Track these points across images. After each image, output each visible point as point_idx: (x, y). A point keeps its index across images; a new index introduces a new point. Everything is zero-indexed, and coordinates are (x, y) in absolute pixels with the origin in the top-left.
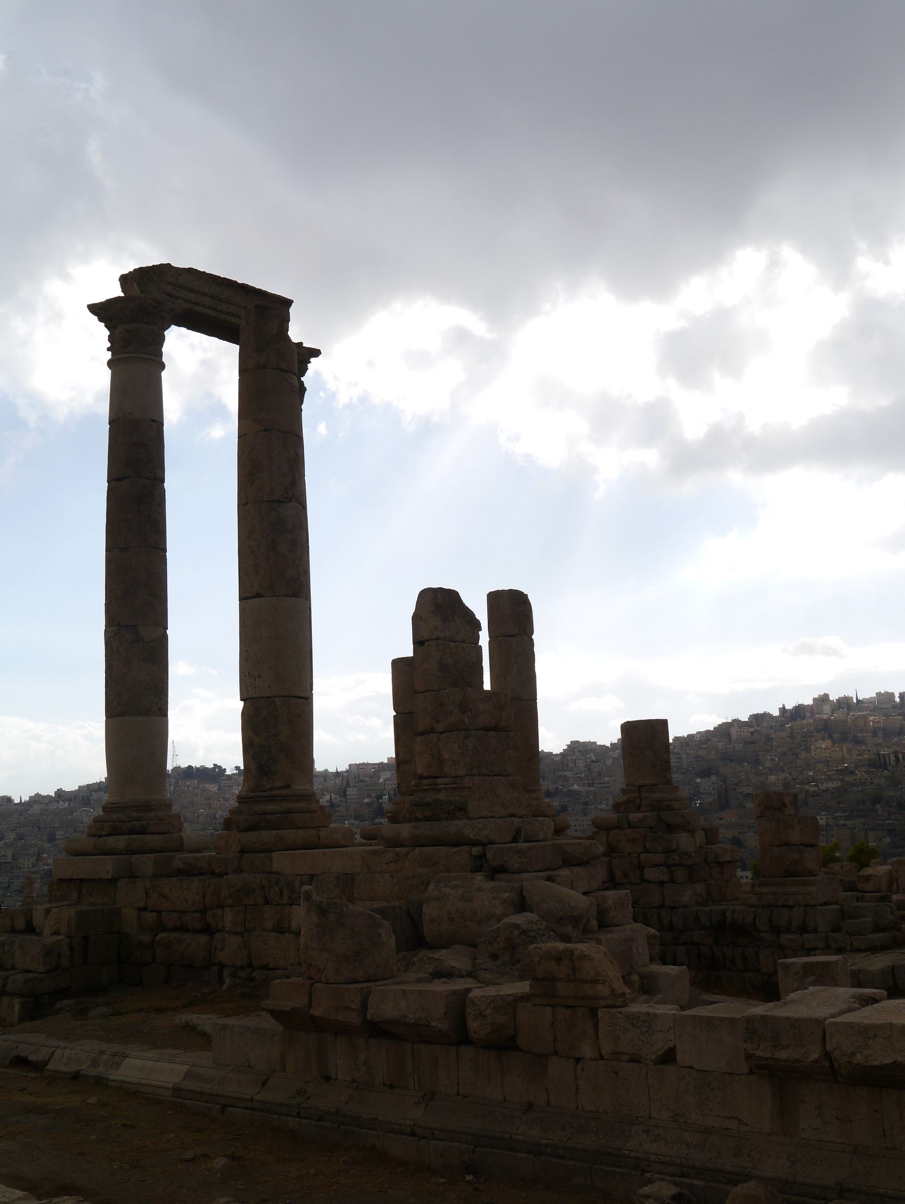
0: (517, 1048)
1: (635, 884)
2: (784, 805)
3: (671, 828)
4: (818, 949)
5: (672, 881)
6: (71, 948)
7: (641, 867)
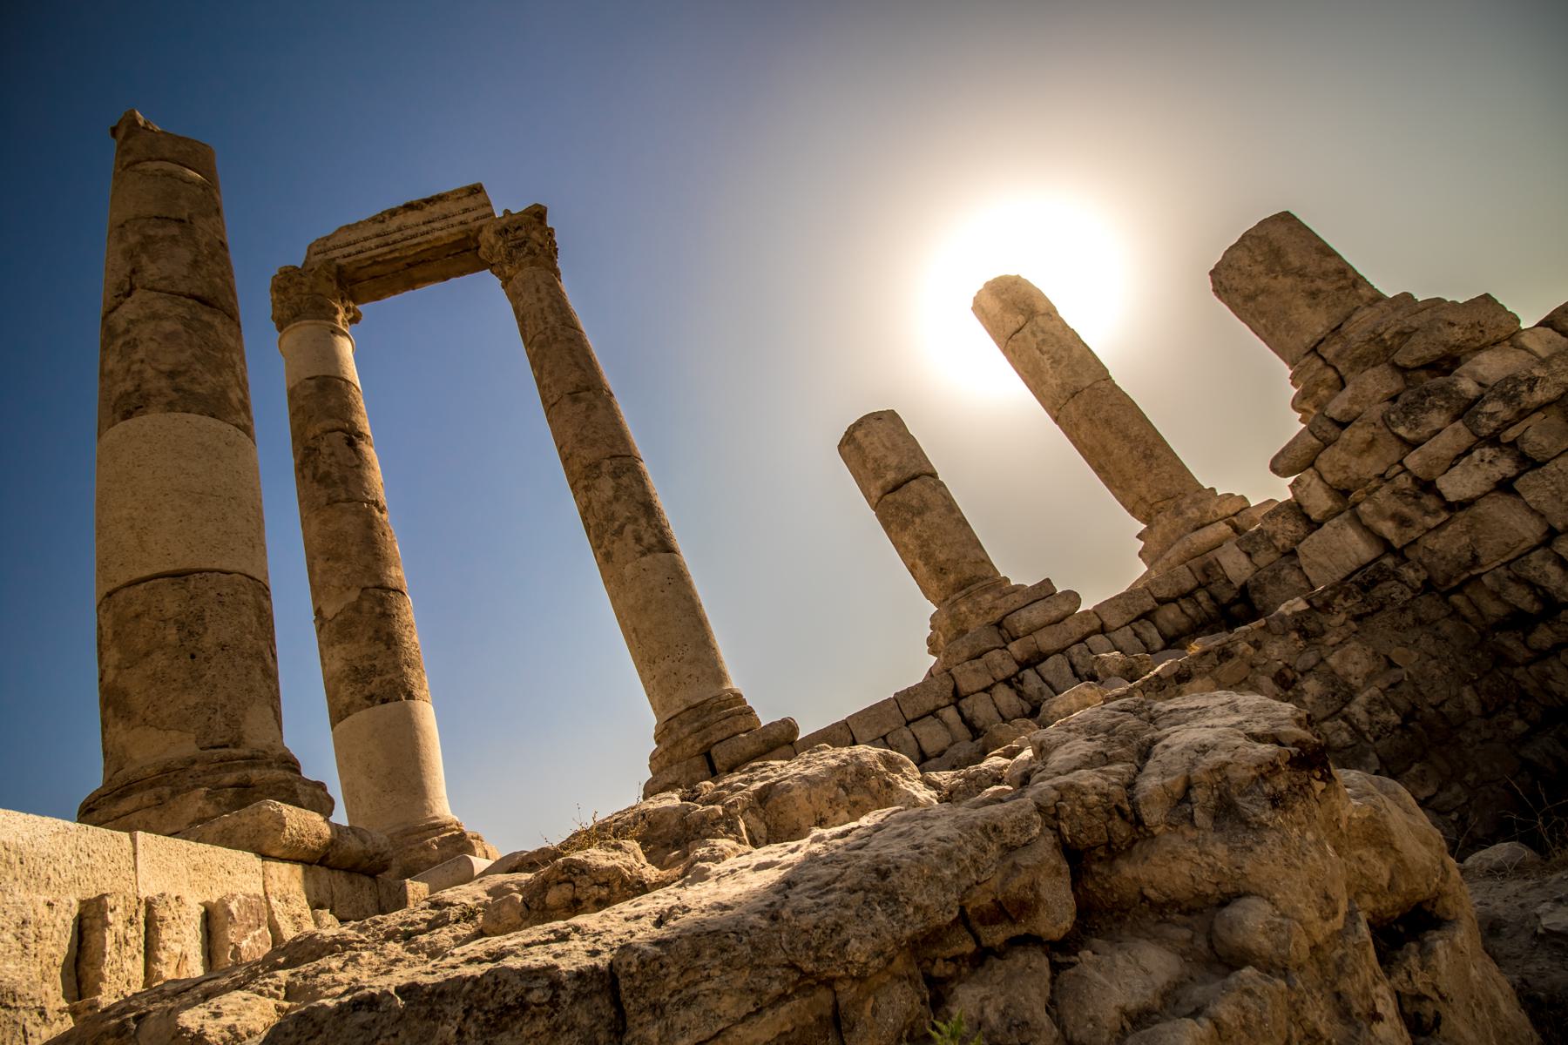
1: (1439, 527)
3: (1447, 363)
5: (1528, 463)
7: (1426, 486)
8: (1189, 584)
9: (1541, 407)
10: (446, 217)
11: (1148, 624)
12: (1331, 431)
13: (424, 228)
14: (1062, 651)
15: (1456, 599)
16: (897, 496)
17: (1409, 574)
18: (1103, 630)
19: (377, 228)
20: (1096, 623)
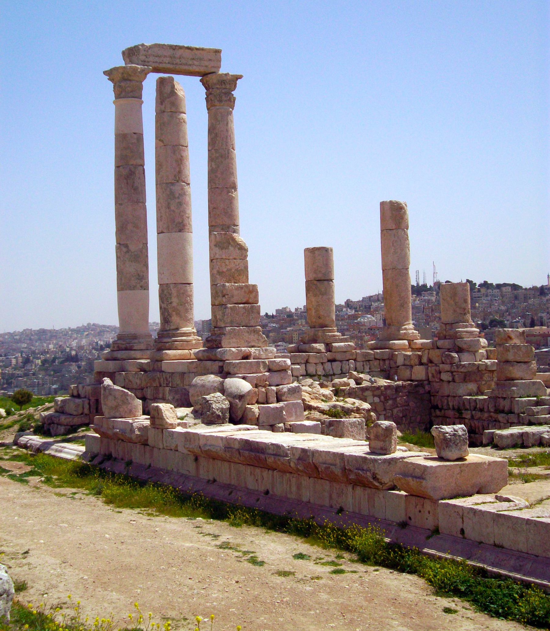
0: (148, 445)
1: (437, 382)
2: (510, 338)
4: (514, 423)
5: (454, 381)
6: (89, 404)
7: (440, 372)
8: (385, 357)
9: (461, 372)
10: (201, 59)
11: (368, 363)
12: (436, 347)
13: (190, 62)
14: (341, 361)
15: (432, 398)
16: (318, 284)
17: (427, 387)
18: (355, 360)
19: (171, 52)
20: (354, 357)
